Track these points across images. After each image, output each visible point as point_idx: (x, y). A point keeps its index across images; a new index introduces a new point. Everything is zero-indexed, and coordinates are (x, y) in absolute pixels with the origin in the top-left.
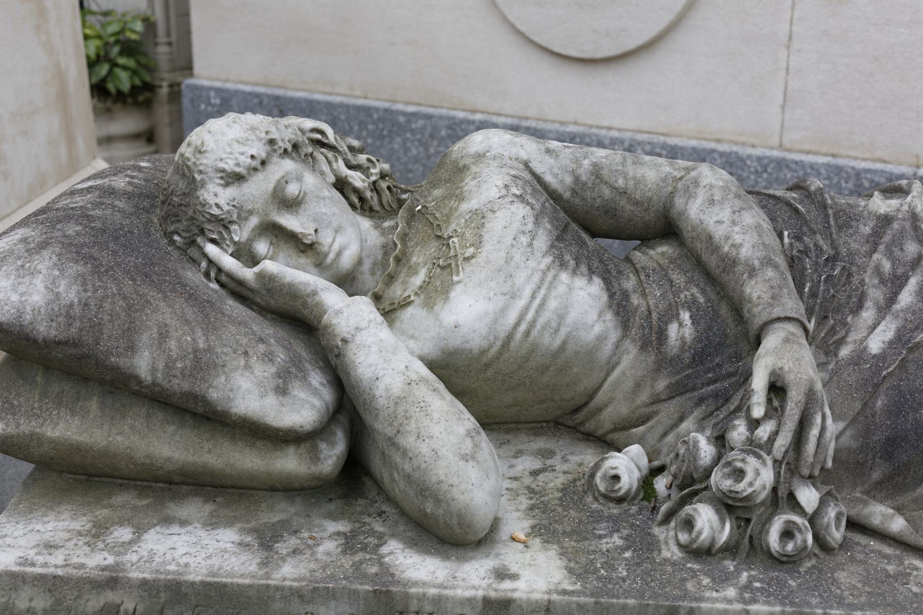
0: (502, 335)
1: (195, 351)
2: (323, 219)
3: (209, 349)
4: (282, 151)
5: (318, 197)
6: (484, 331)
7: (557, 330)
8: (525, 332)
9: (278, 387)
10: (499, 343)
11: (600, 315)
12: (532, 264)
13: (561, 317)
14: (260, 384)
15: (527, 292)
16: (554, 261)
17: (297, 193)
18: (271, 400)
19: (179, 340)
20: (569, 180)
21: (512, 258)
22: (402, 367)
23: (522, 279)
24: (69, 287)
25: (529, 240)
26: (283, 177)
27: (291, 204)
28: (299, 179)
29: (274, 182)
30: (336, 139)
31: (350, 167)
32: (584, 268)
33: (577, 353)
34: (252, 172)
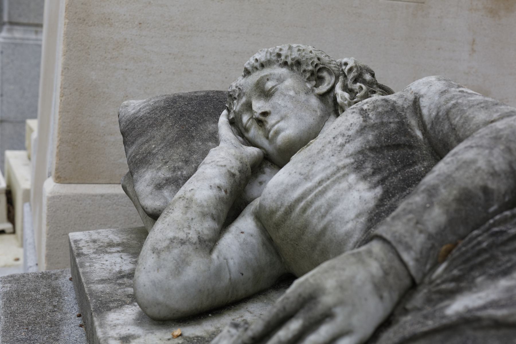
0: (286, 204)
1: (149, 153)
2: (277, 108)
3: (154, 155)
4: (281, 62)
5: (282, 93)
6: (275, 196)
7: (323, 216)
8: (302, 208)
9: (159, 184)
10: (283, 209)
11: (358, 216)
12: (334, 159)
13: (330, 207)
14: (152, 179)
15: (317, 179)
16: (353, 164)
17: (270, 87)
18: (149, 189)
19: (148, 147)
20: (434, 114)
21: (324, 150)
22: (190, 189)
23: (319, 168)
24: (147, 109)
25: (343, 142)
26: (266, 76)
27: (266, 94)
28: (280, 80)
29: (259, 77)
30: (351, 70)
31: (345, 88)
32: (377, 178)
33: (331, 241)
34: (255, 70)
